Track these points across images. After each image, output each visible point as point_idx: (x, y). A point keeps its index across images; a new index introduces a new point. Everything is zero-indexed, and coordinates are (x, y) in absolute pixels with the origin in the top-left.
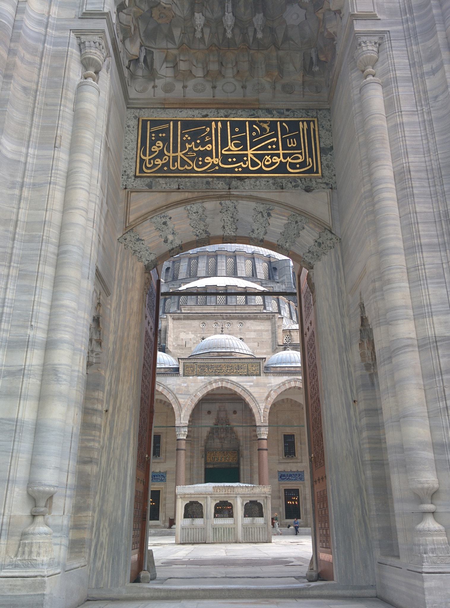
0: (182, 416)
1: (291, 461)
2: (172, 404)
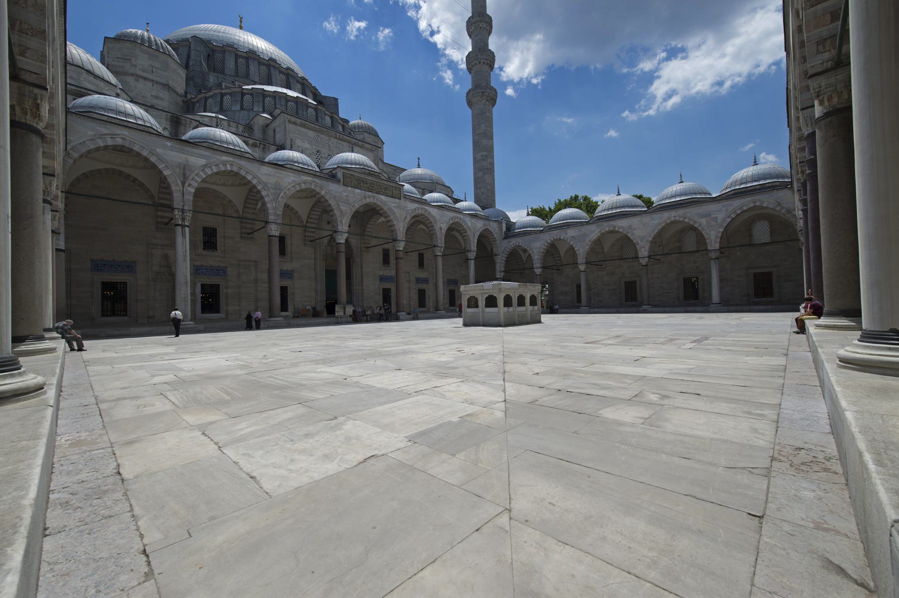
0: (344, 222)
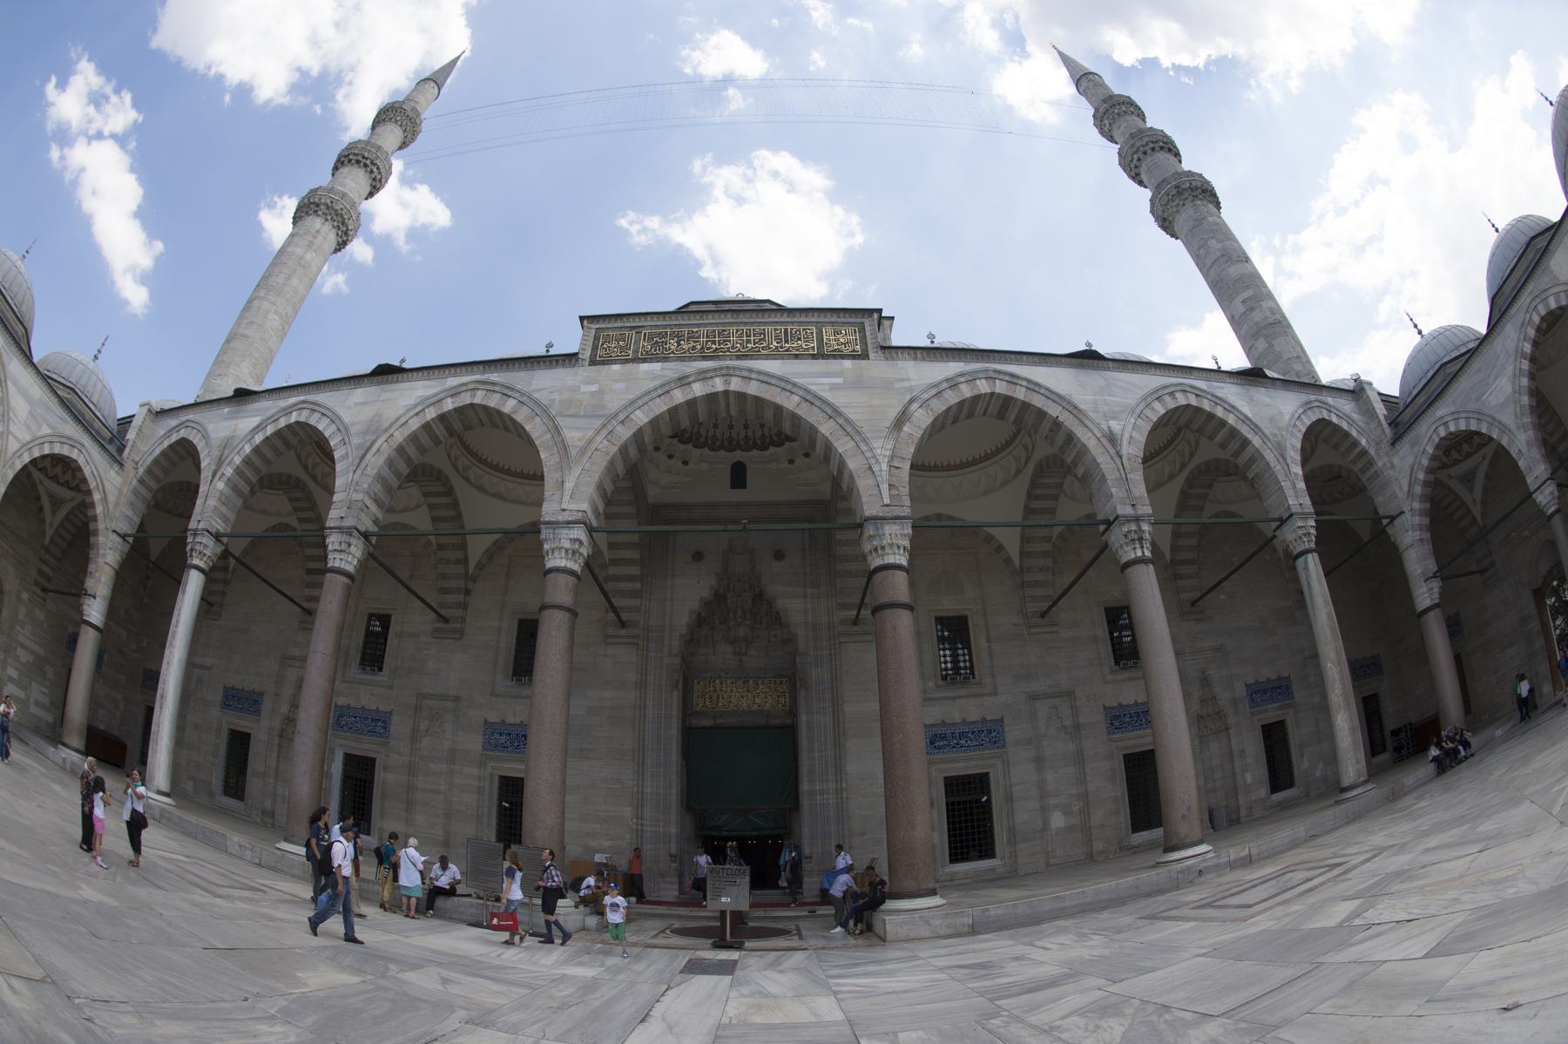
0: (569, 485)
1: (964, 692)
2: (541, 449)
